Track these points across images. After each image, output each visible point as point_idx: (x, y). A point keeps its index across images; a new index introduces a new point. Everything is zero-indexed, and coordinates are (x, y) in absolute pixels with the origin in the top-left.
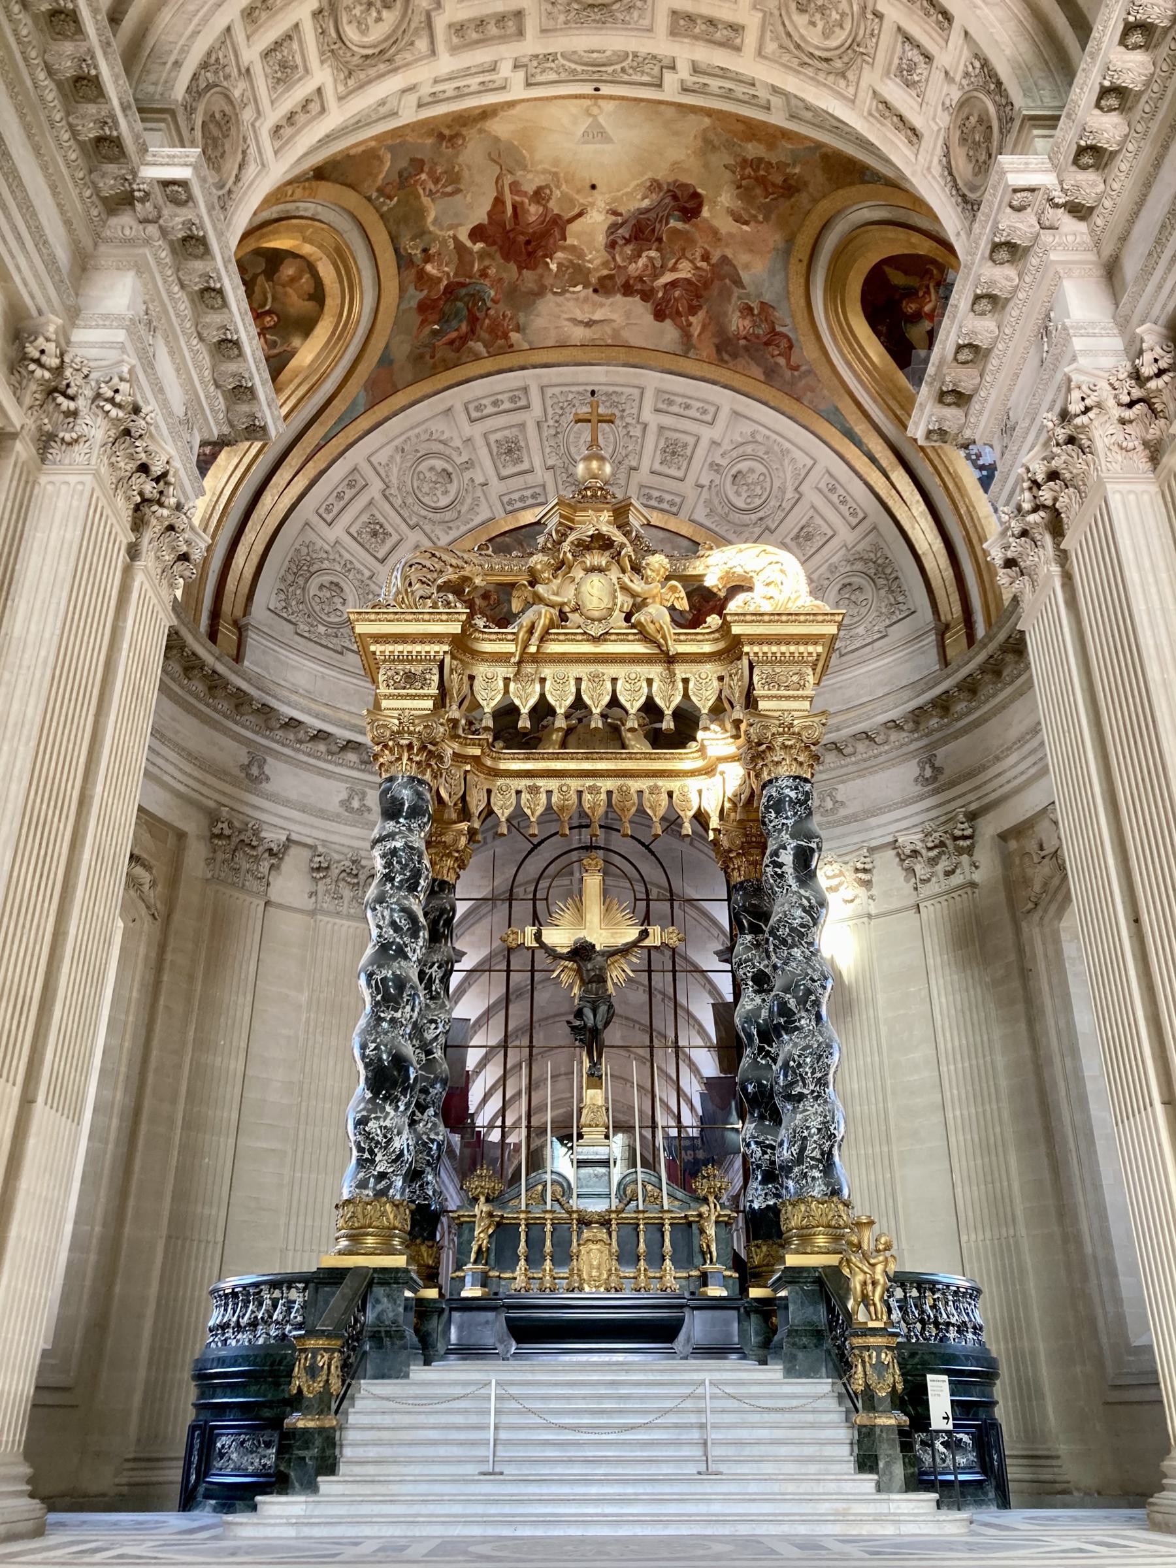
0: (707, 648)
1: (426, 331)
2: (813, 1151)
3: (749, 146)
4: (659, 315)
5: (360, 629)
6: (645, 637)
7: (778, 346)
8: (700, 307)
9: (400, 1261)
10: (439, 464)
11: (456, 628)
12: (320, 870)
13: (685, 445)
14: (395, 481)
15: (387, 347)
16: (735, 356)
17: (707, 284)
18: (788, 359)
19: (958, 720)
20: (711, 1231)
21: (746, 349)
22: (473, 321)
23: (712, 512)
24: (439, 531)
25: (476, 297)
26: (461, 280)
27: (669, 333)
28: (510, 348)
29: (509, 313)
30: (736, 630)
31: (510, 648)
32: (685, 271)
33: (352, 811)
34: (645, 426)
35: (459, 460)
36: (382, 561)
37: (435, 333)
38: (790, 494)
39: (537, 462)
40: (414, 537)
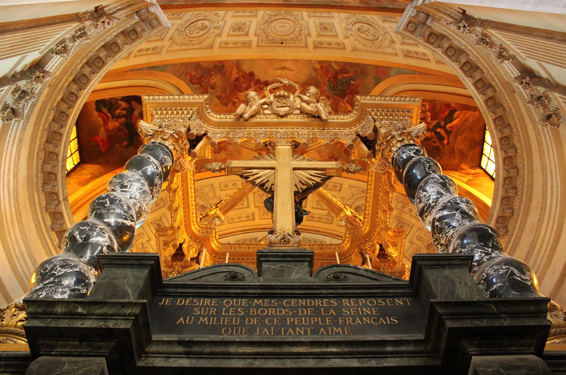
1: (357, 82)
3: (224, 156)
4: (252, 74)
7: (197, 78)
8: (234, 81)
10: (363, 35)
13: (233, 31)
15: (376, 85)
16: (216, 66)
17: (232, 92)
18: (191, 76)
19: (50, 110)
21: (210, 71)
22: (336, 78)
25: (333, 88)
26: (338, 98)
27: (247, 69)
28: (320, 62)
29: (319, 77)
37: (353, 80)
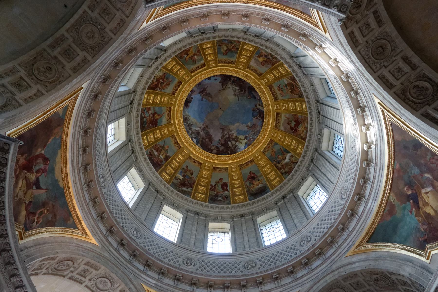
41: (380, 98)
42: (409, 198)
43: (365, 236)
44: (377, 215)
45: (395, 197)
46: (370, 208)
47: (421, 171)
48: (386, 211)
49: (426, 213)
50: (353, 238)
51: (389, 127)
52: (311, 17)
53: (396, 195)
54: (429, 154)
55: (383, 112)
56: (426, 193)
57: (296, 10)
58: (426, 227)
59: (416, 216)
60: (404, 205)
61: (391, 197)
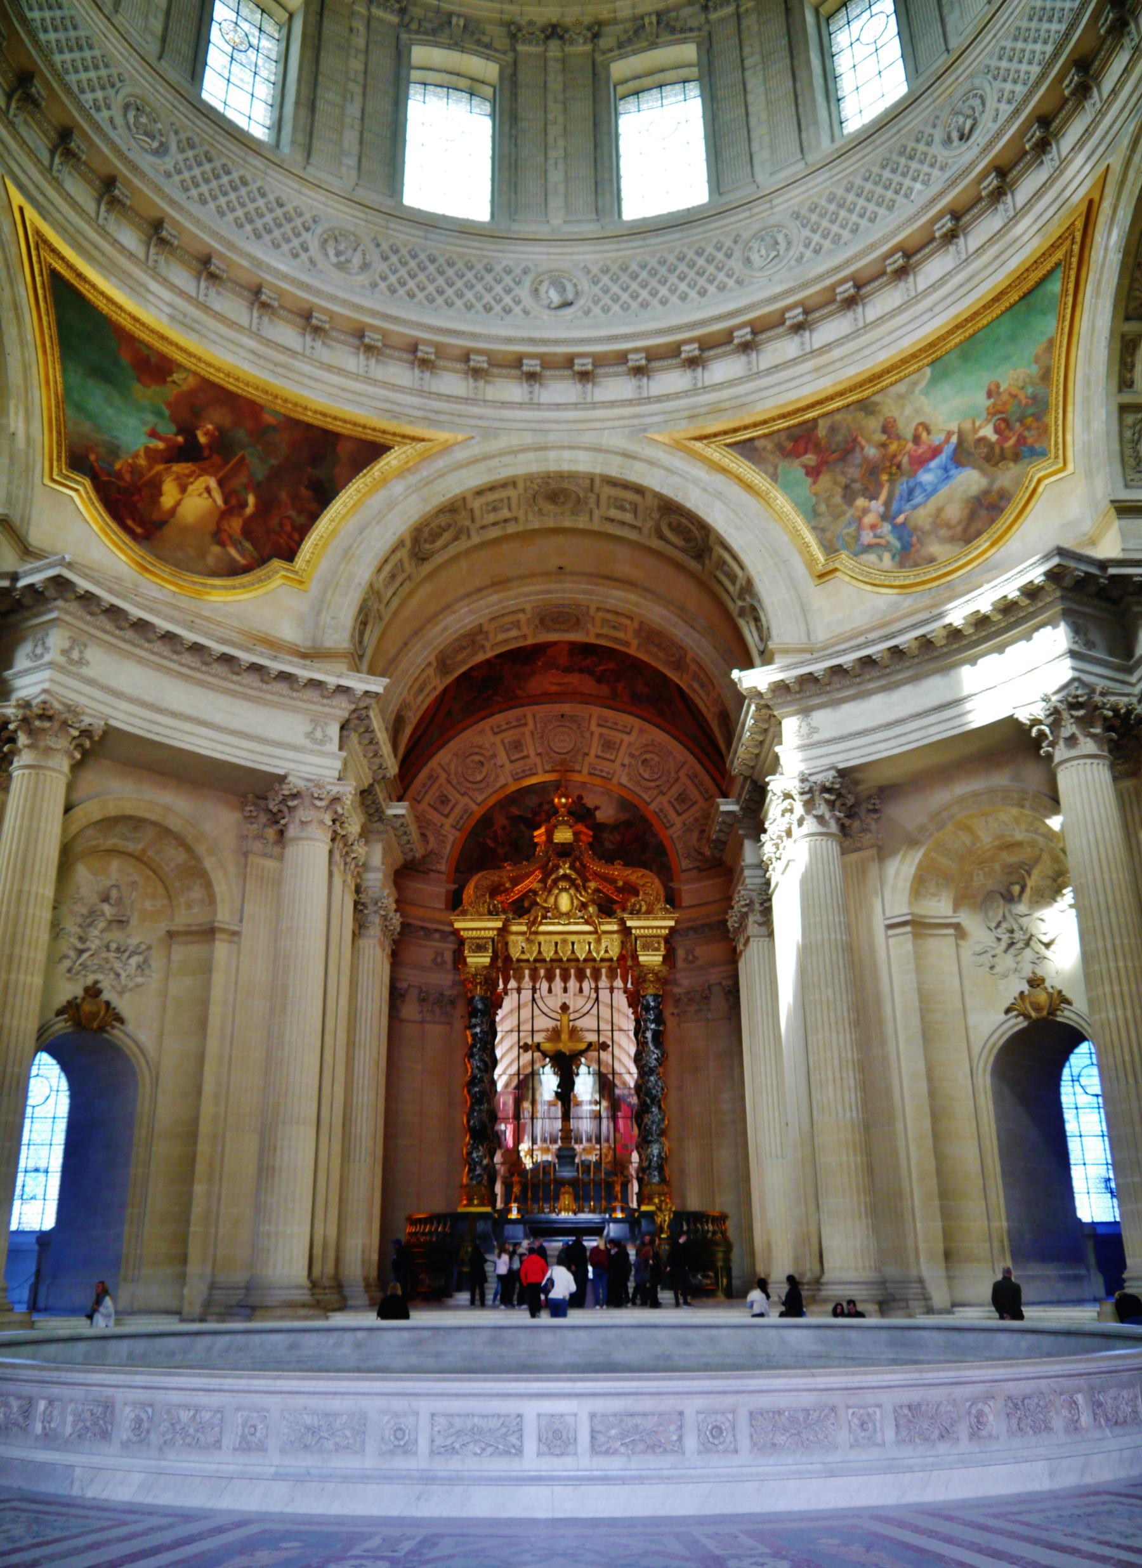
0: (615, 927)
2: (654, 1164)
4: (599, 681)
5: (457, 925)
6: (587, 923)
9: (488, 1209)
10: (477, 758)
11: (499, 924)
12: (422, 1000)
14: (452, 770)
20: (618, 1188)
23: (630, 779)
24: (476, 794)
27: (604, 690)
30: (629, 924)
31: (524, 928)
32: (611, 666)
33: (438, 963)
34: (592, 733)
35: (488, 754)
36: (447, 816)
38: (673, 775)
39: (532, 753)
40: (466, 800)
41: (461, 455)
42: (188, 431)
43: (70, 266)
44: (136, 319)
45: (185, 388)
46: (148, 290)
47: (259, 484)
48: (146, 352)
49: (161, 482)
50: (59, 212)
51: (380, 439)
52: (729, 445)
53: (192, 393)
54: (302, 520)
55: (423, 440)
56: (208, 490)
57: (765, 436)
58: (127, 477)
59: (147, 449)
60: (167, 412)
61: (183, 376)
